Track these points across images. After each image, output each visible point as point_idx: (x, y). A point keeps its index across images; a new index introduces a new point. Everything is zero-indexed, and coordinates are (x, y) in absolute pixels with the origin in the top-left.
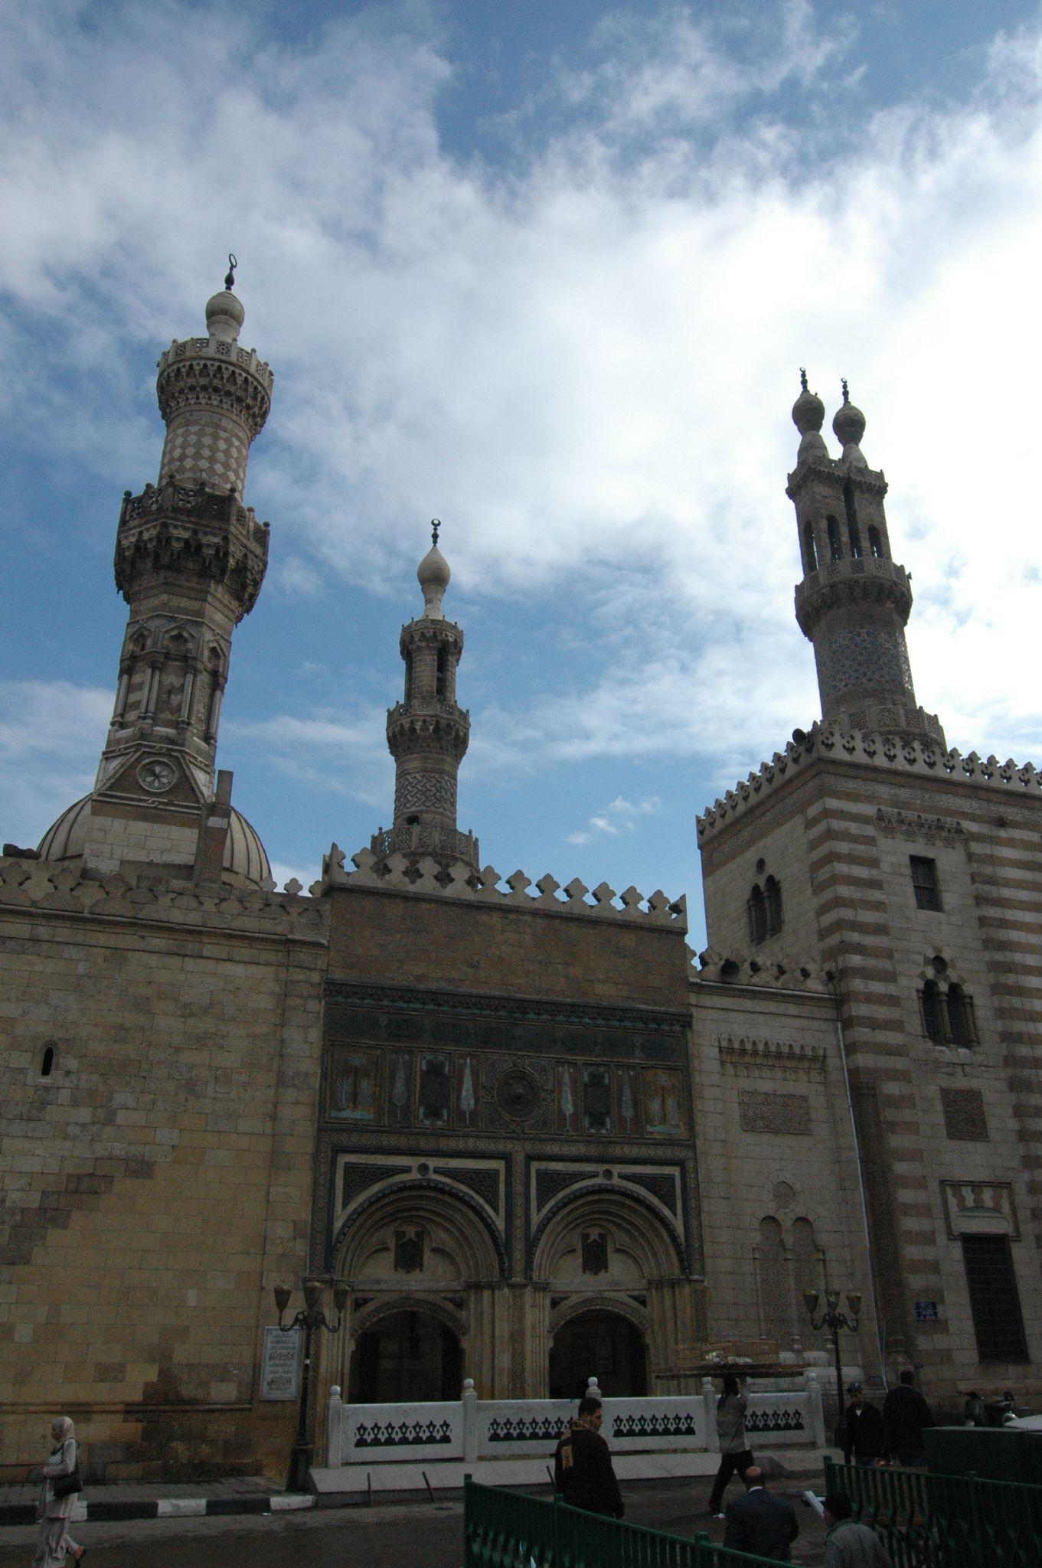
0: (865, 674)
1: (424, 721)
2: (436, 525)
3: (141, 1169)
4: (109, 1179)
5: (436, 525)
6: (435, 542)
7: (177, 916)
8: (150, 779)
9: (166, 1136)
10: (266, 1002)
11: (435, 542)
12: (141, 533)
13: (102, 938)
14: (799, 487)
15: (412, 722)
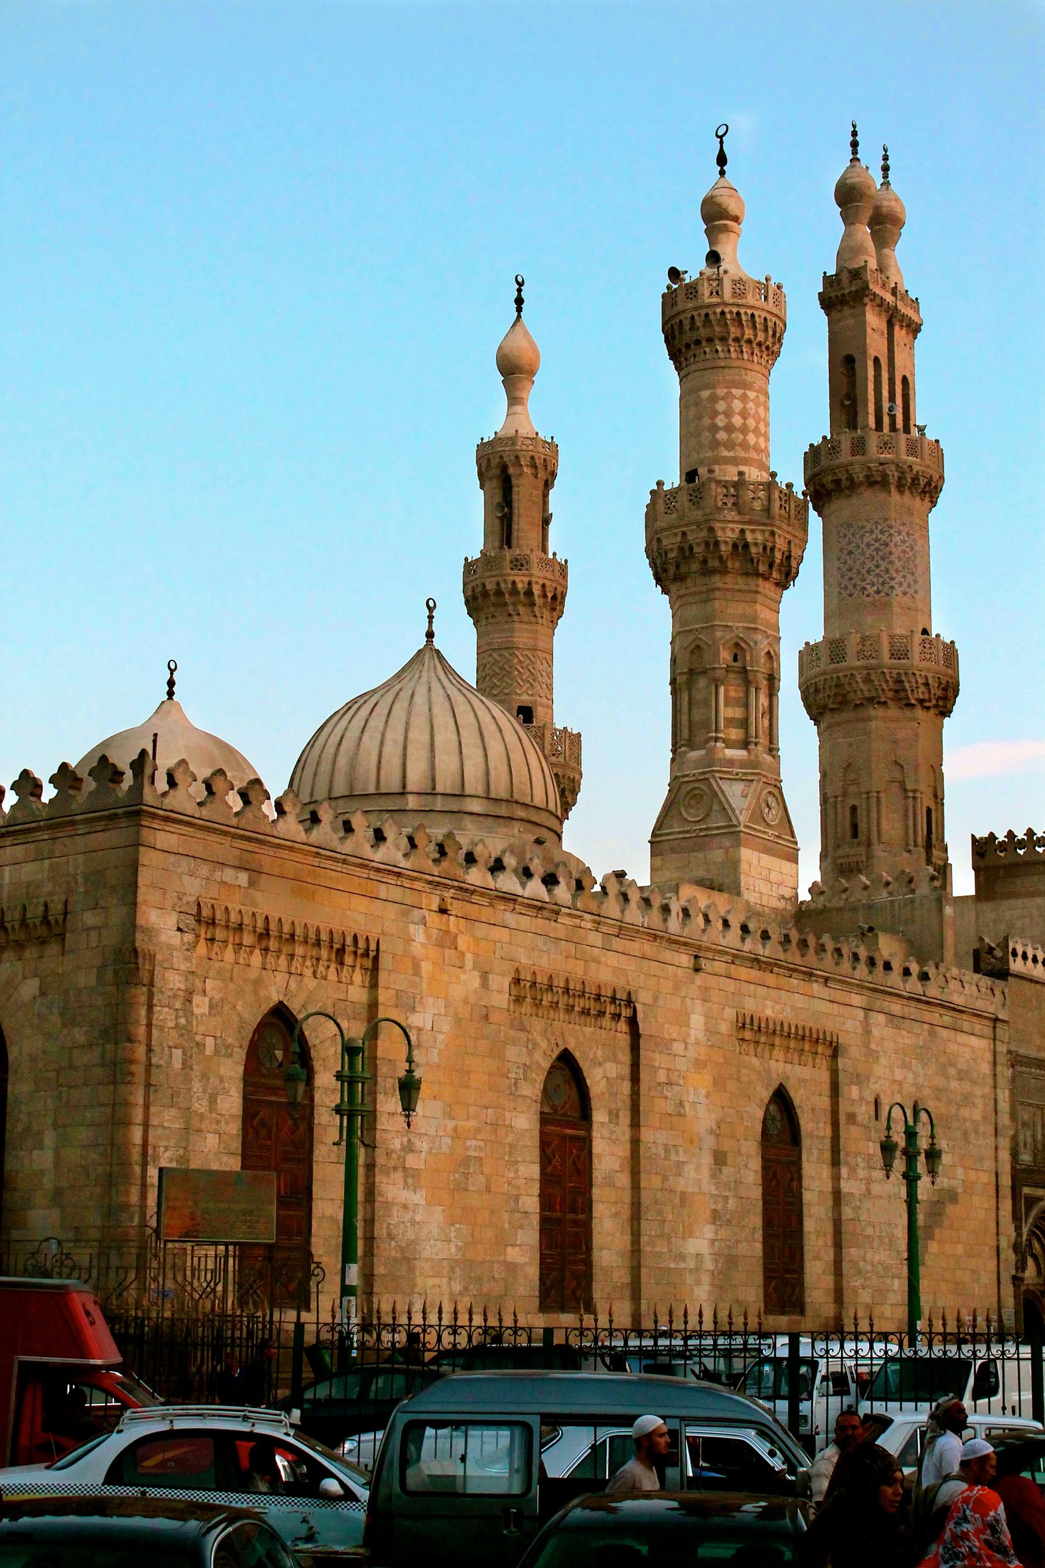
0: (901, 584)
1: (543, 586)
2: (520, 284)
3: (952, 1196)
4: (944, 1203)
5: (520, 284)
6: (519, 310)
7: (958, 1000)
8: (766, 810)
9: (959, 1172)
10: (986, 1068)
11: (519, 310)
12: (742, 531)
13: (927, 1016)
14: (843, 301)
15: (530, 583)
